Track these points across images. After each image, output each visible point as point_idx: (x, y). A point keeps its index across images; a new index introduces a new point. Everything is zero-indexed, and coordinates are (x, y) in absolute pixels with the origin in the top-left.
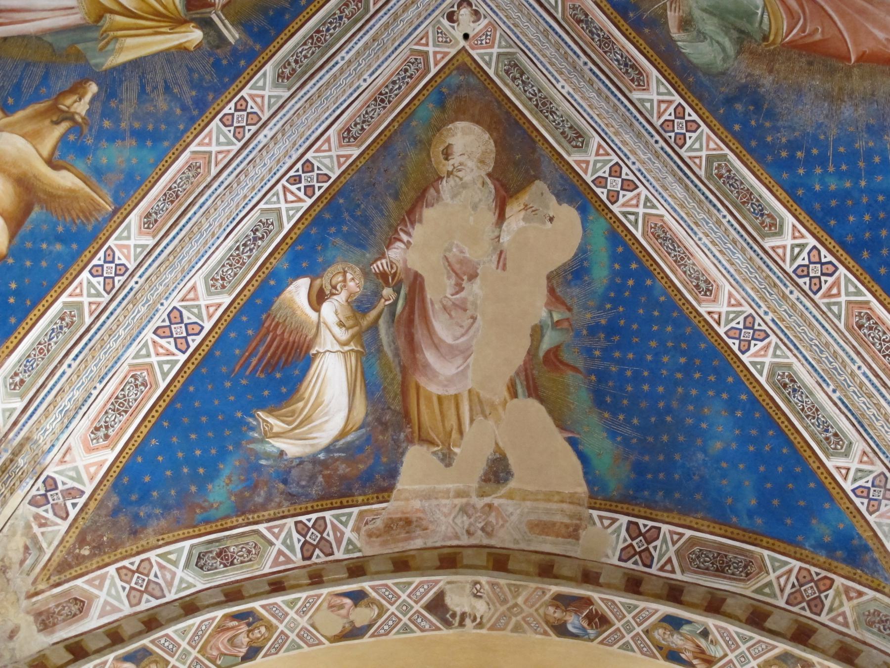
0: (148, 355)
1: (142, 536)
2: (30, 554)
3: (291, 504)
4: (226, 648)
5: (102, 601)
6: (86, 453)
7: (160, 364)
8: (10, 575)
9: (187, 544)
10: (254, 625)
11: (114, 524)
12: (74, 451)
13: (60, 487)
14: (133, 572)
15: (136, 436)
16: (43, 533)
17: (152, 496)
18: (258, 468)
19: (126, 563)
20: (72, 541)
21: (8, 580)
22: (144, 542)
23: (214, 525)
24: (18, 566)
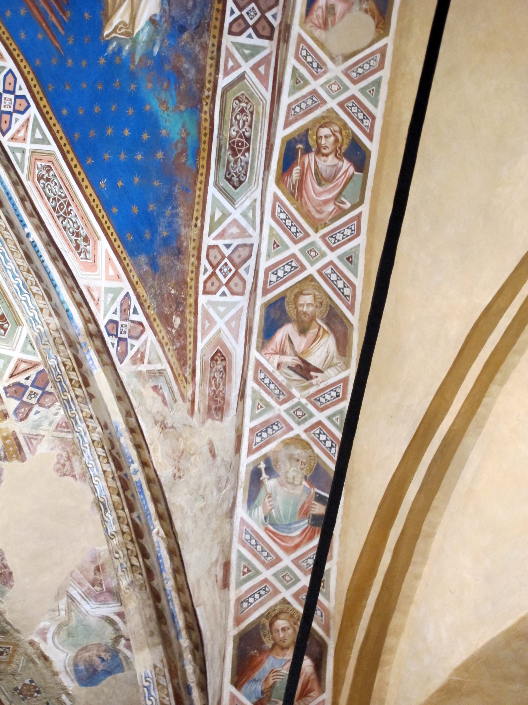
0: (23, 151)
1: (185, 244)
2: (161, 388)
3: (208, 30)
4: (329, 191)
5: (224, 328)
6: (95, 270)
7: (35, 141)
8: (169, 423)
9: (212, 189)
10: (312, 143)
11: (164, 273)
12: (92, 285)
13: (117, 318)
14: (214, 273)
15: (92, 203)
16: (149, 363)
17: (152, 212)
18: (161, 59)
19: (202, 278)
20: (164, 333)
21: (172, 427)
22: (192, 245)
23: (203, 146)
24: (165, 408)
